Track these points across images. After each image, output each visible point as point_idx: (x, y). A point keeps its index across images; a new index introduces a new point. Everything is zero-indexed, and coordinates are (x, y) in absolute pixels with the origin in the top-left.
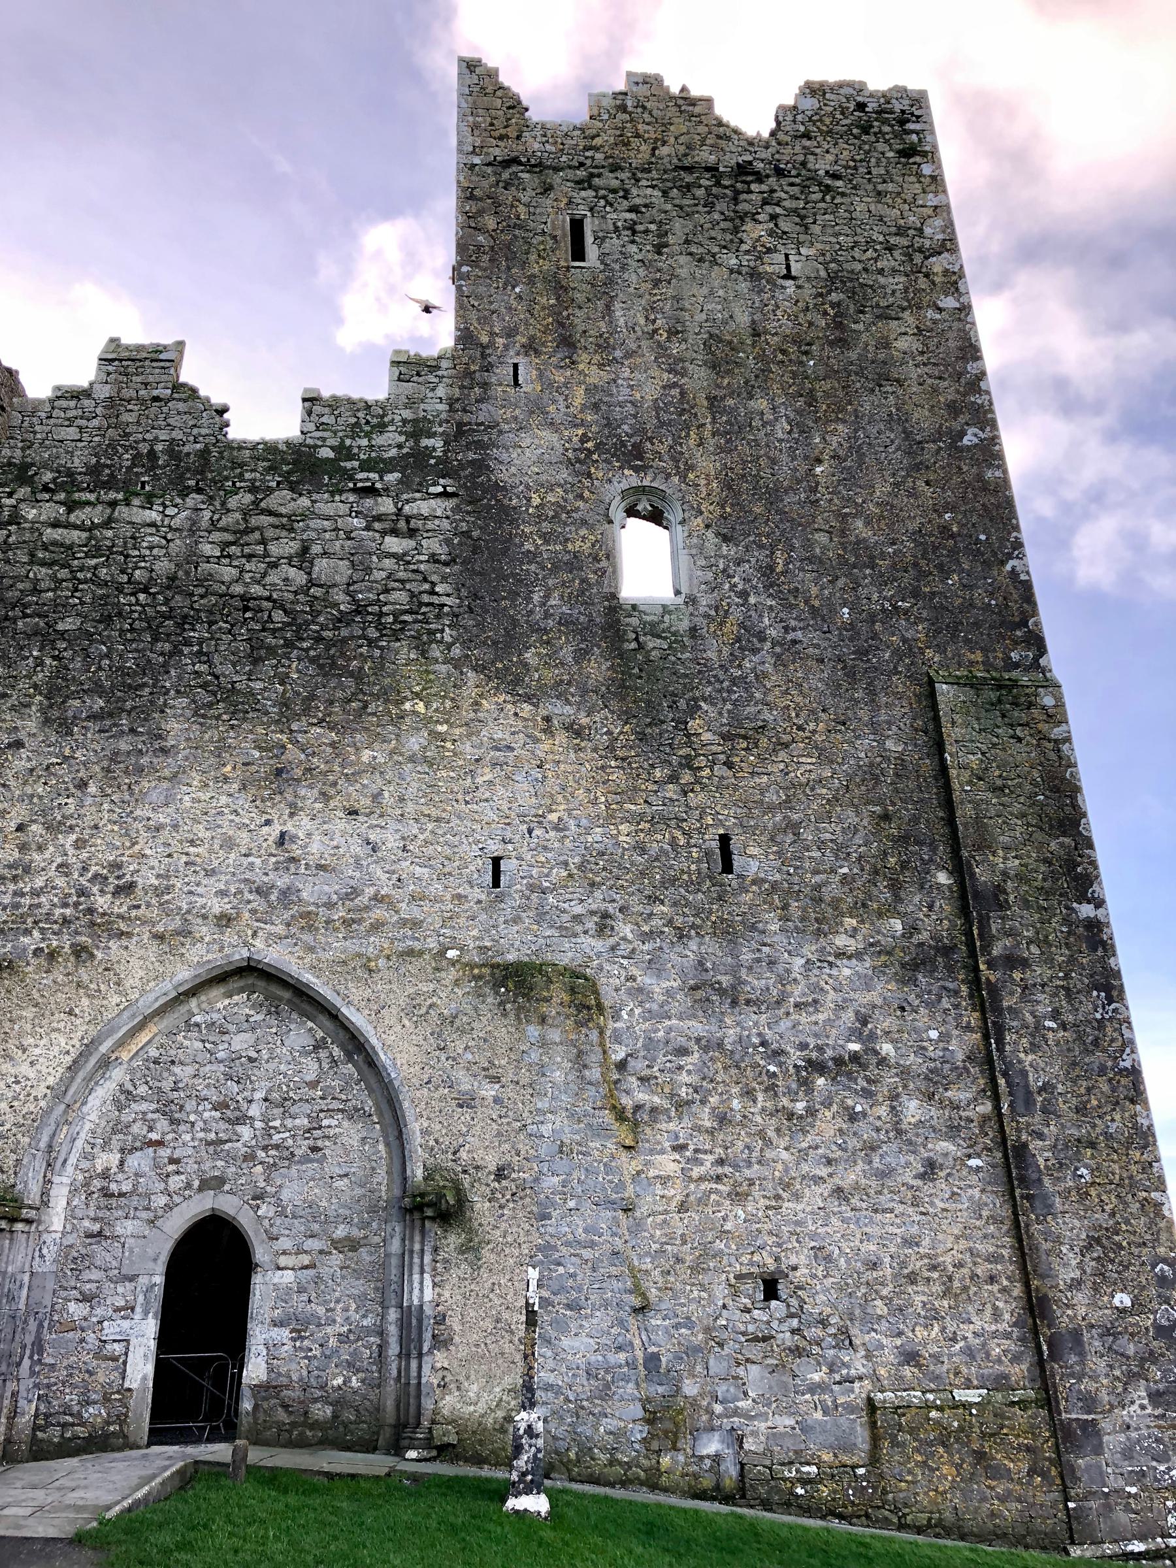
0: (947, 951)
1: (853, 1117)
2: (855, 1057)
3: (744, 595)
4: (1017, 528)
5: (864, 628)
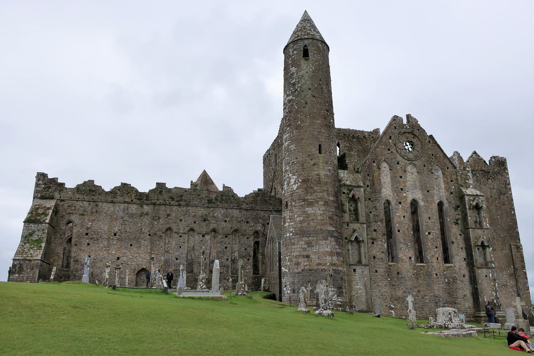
0: (513, 274)
1: (506, 290)
2: (506, 285)
3: (493, 233)
4: (517, 225)
5: (504, 237)
